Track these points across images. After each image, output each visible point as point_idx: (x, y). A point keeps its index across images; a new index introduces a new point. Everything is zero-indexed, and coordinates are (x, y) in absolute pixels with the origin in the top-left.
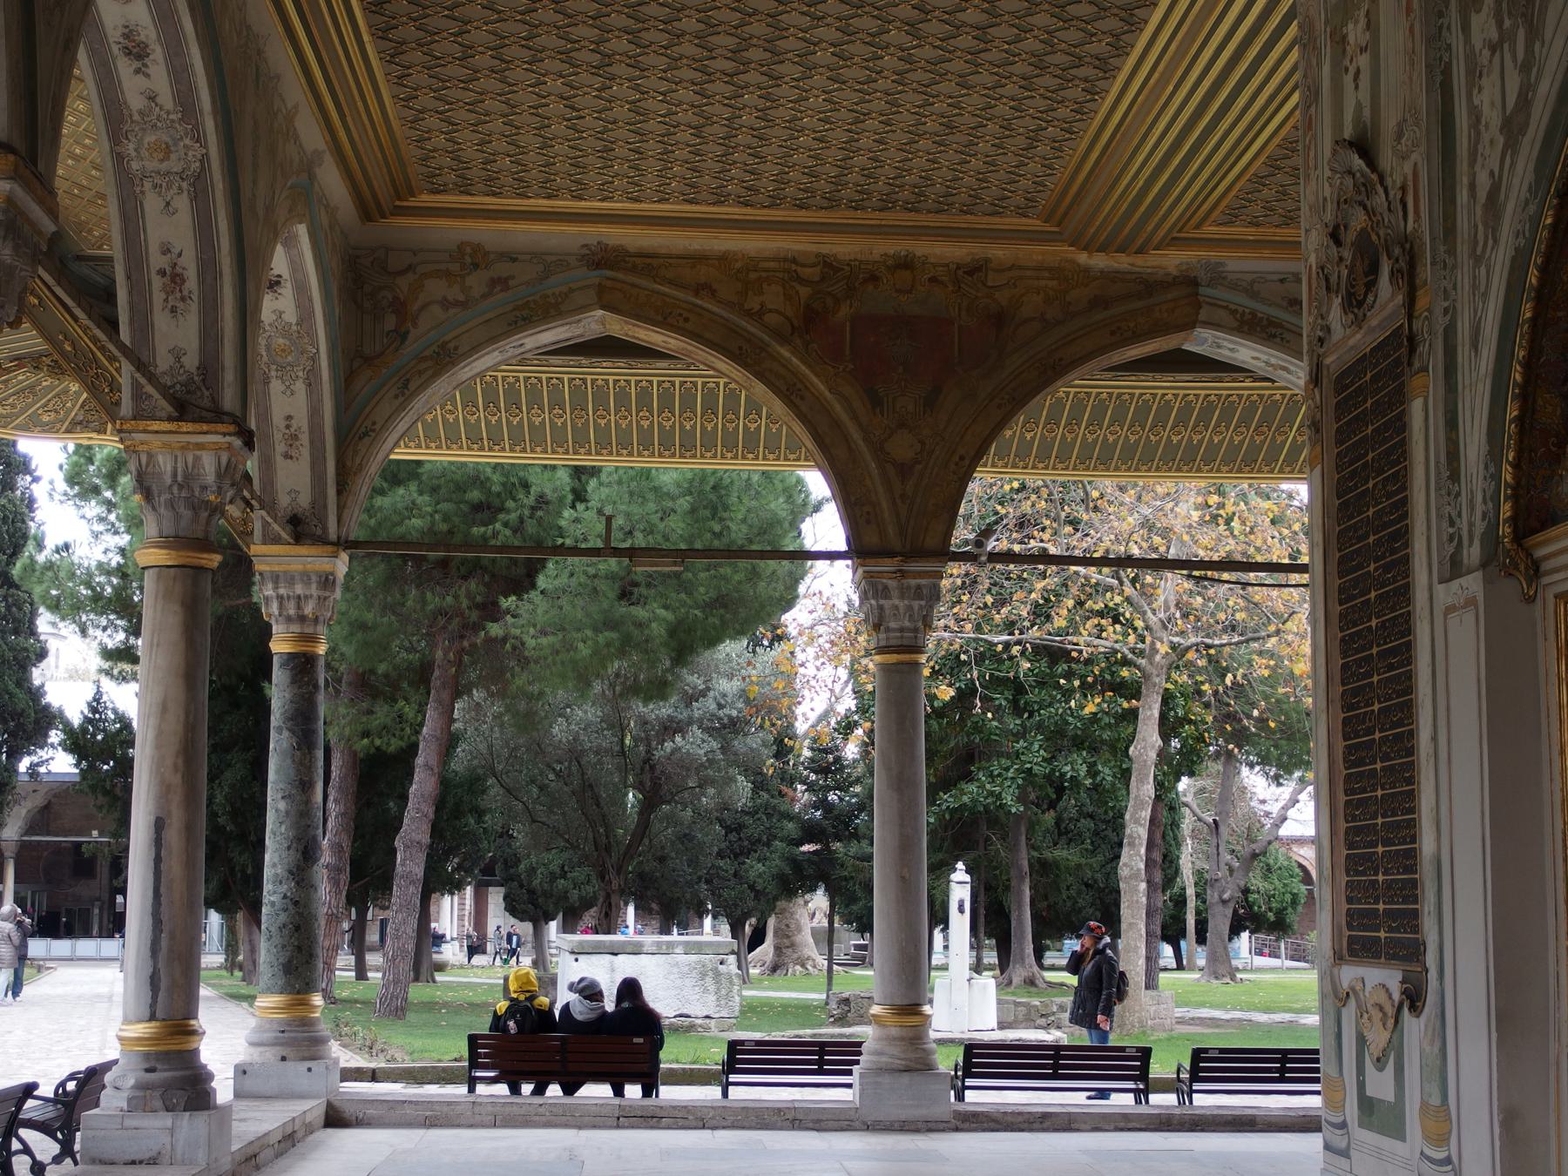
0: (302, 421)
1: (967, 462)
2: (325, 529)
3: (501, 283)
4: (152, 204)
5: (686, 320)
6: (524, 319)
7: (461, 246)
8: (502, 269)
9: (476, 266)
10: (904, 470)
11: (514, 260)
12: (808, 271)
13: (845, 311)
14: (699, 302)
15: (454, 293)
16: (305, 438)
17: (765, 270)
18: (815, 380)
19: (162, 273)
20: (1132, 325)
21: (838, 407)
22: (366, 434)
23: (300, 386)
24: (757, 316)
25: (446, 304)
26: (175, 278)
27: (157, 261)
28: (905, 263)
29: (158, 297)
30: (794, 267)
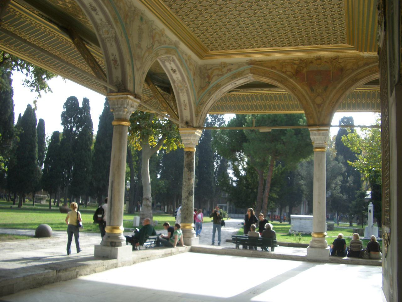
0: (187, 101)
1: (334, 103)
2: (193, 124)
3: (230, 70)
4: (108, 45)
5: (270, 75)
6: (235, 77)
7: (221, 63)
8: (229, 67)
9: (224, 67)
10: (319, 106)
11: (232, 65)
12: (296, 62)
13: (305, 70)
14: (272, 71)
15: (220, 73)
16: (188, 105)
17: (287, 62)
18: (299, 86)
19: (113, 60)
20: (375, 69)
21: (304, 92)
22: (202, 104)
23: (185, 94)
24: (285, 72)
25: (218, 75)
26: (115, 61)
27: (112, 58)
28: (319, 58)
29: (113, 66)
30: (293, 61)
